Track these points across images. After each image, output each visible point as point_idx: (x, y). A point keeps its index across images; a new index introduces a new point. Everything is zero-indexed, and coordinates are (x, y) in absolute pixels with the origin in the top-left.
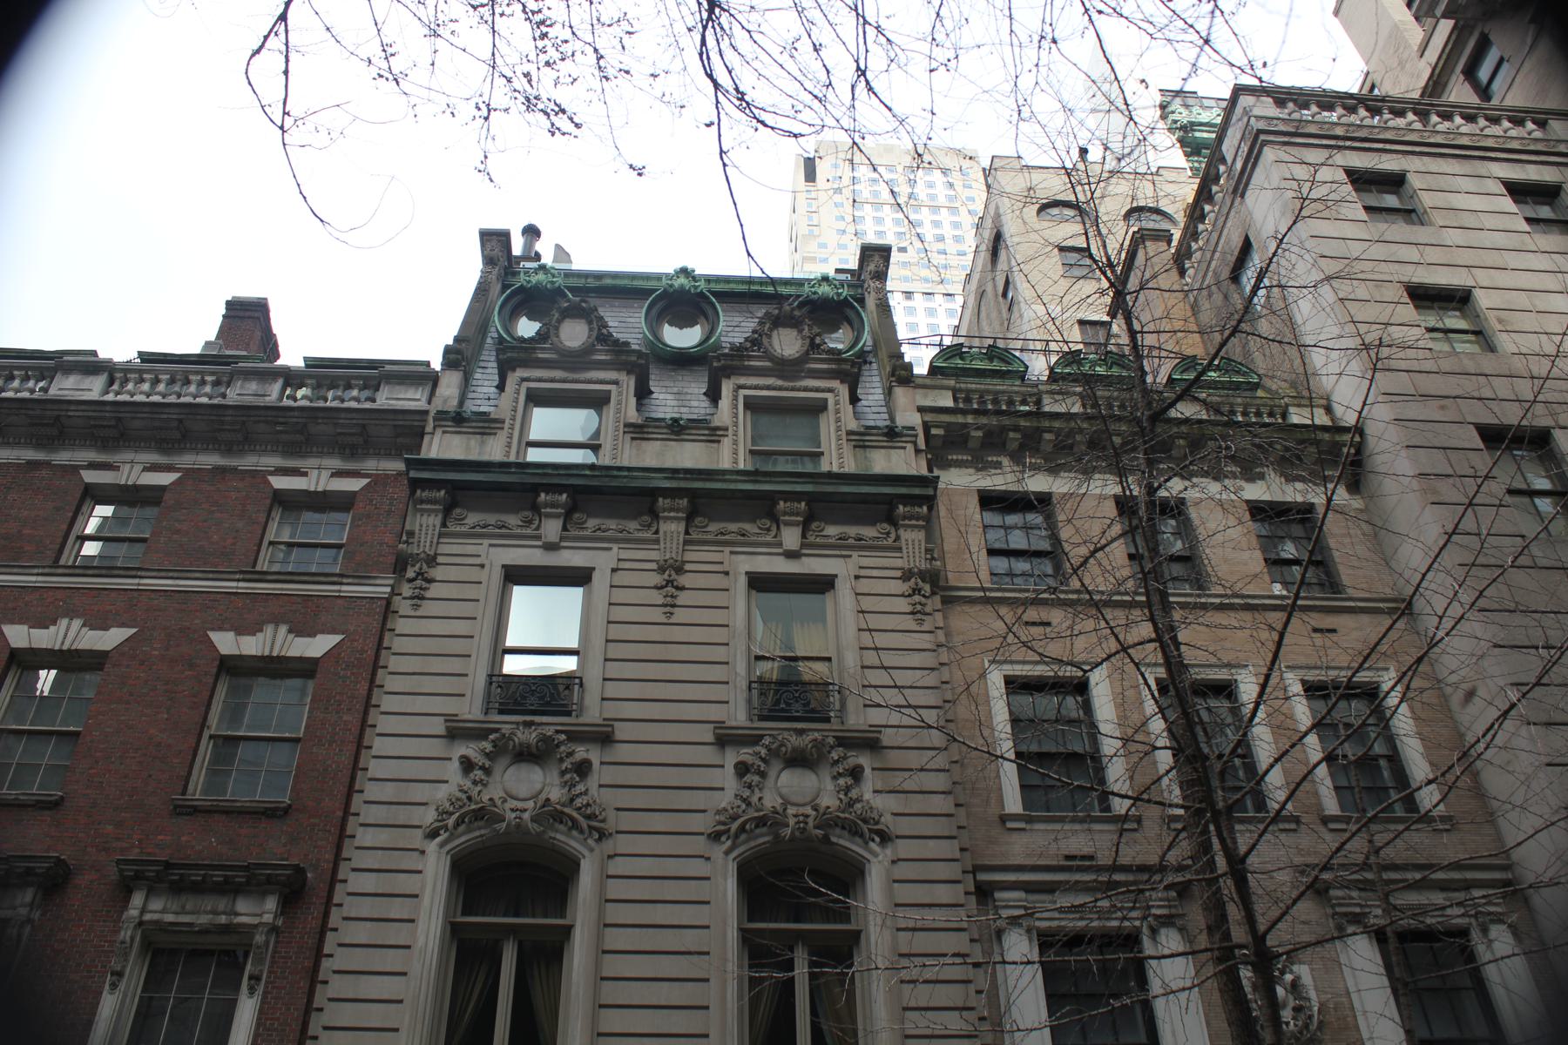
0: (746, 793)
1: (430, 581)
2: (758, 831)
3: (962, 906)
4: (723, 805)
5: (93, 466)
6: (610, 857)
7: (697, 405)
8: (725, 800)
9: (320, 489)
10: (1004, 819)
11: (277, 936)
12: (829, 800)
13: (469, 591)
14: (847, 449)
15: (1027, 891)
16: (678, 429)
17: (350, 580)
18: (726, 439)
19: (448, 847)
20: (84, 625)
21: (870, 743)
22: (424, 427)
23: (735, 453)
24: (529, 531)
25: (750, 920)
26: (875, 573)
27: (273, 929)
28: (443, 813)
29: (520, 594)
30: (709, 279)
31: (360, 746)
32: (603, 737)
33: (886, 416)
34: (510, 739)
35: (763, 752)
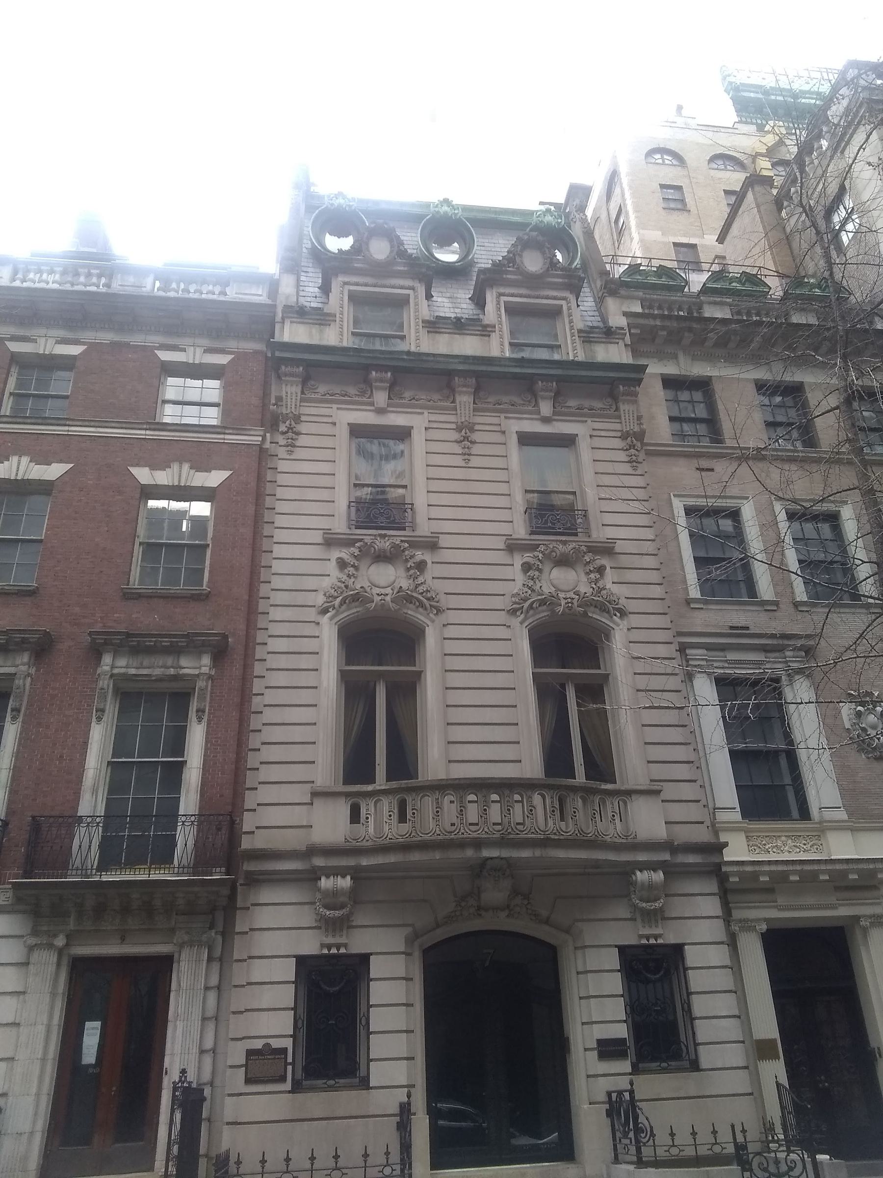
0: (531, 583)
1: (298, 434)
2: (540, 608)
3: (674, 659)
5: (14, 338)
7: (464, 308)
8: (517, 587)
9: (197, 362)
10: (688, 602)
11: (212, 682)
12: (584, 588)
16: (459, 326)
17: (231, 431)
20: (31, 461)
21: (607, 550)
22: (274, 316)
26: (603, 433)
27: (210, 677)
28: (331, 598)
30: (466, 208)
32: (433, 545)
34: (371, 546)
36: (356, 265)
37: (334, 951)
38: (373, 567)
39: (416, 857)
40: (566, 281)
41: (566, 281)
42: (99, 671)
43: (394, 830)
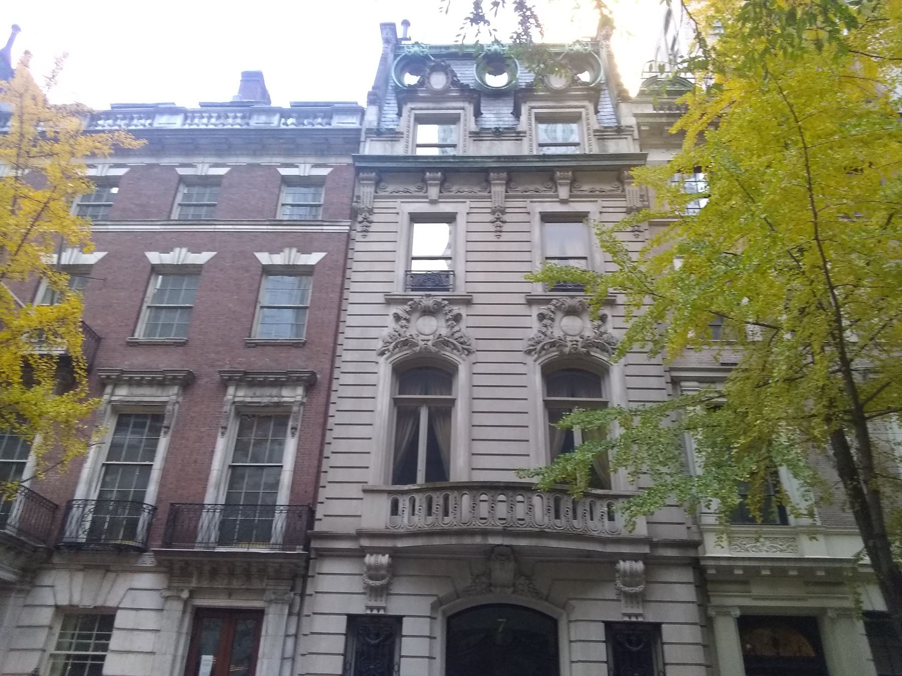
0: (544, 330)
1: (371, 222)
2: (552, 349)
3: (664, 389)
4: (532, 336)
5: (183, 165)
6: (474, 363)
7: (507, 120)
8: (533, 333)
12: (589, 333)
13: (392, 227)
14: (594, 140)
15: (700, 382)
16: (498, 134)
18: (525, 138)
19: (391, 359)
22: (359, 138)
23: (531, 145)
24: (421, 194)
25: (548, 396)
27: (302, 404)
29: (417, 227)
31: (340, 310)
32: (467, 302)
33: (614, 121)
35: (553, 308)
36: (421, 95)
37: (375, 612)
38: (421, 320)
39: (437, 541)
40: (585, 93)
41: (585, 93)
42: (225, 399)
43: (421, 521)
